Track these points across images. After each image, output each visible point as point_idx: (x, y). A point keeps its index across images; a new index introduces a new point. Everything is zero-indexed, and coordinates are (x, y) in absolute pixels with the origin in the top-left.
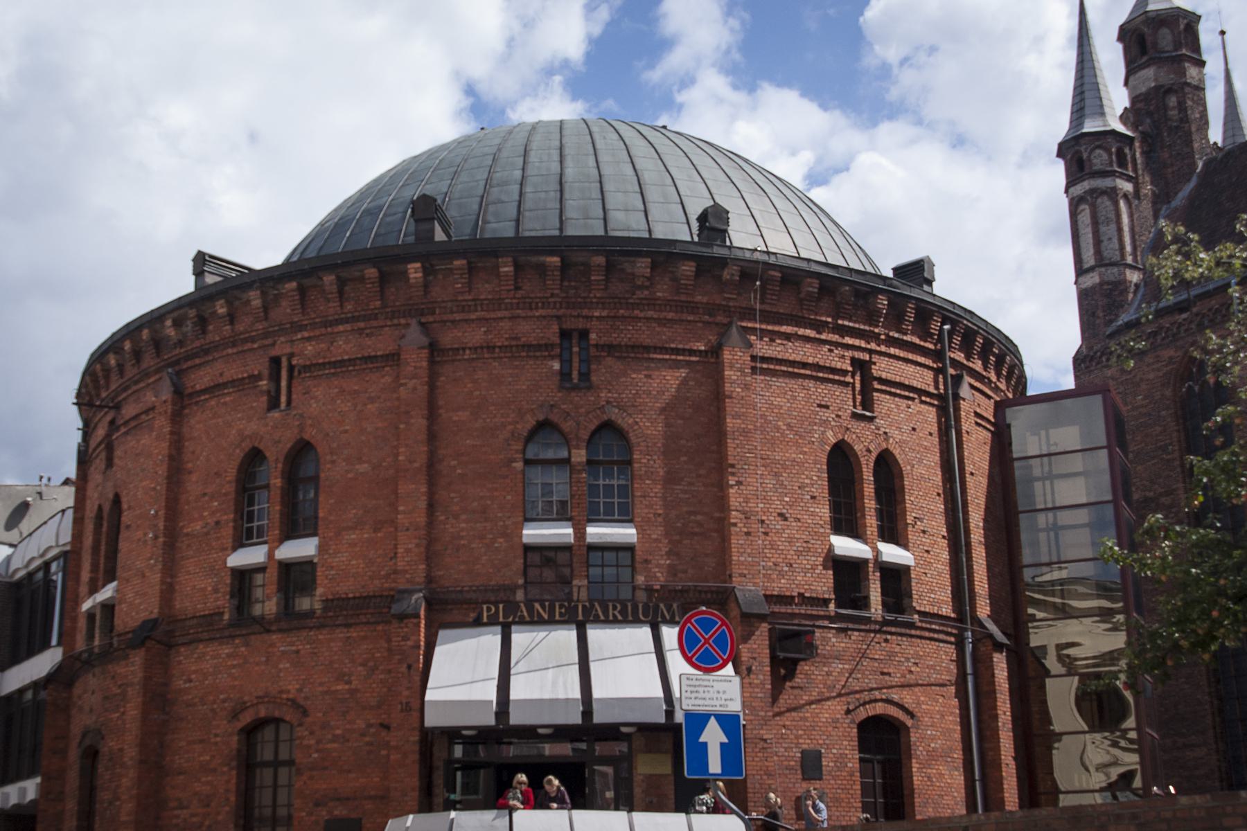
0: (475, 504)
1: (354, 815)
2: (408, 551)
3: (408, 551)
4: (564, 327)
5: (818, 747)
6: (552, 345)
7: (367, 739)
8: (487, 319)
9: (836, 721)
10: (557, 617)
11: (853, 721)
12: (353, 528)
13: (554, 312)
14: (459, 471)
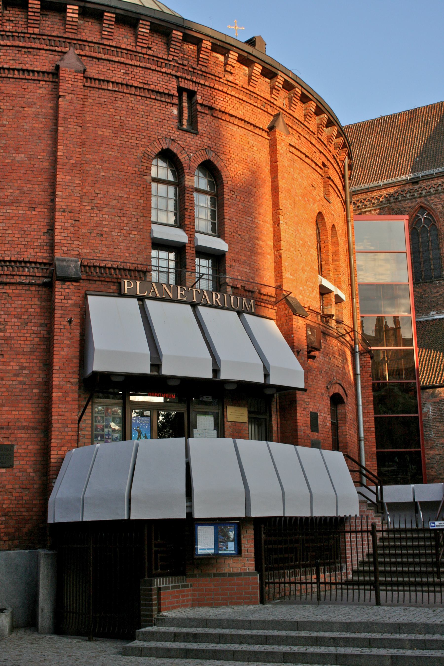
0: (115, 202)
1: (6, 442)
2: (64, 228)
3: (64, 228)
4: (181, 85)
5: (316, 411)
6: (172, 96)
7: (21, 379)
8: (126, 64)
9: (322, 394)
10: (179, 298)
11: (328, 396)
12: (11, 204)
13: (173, 73)
14: (103, 174)
